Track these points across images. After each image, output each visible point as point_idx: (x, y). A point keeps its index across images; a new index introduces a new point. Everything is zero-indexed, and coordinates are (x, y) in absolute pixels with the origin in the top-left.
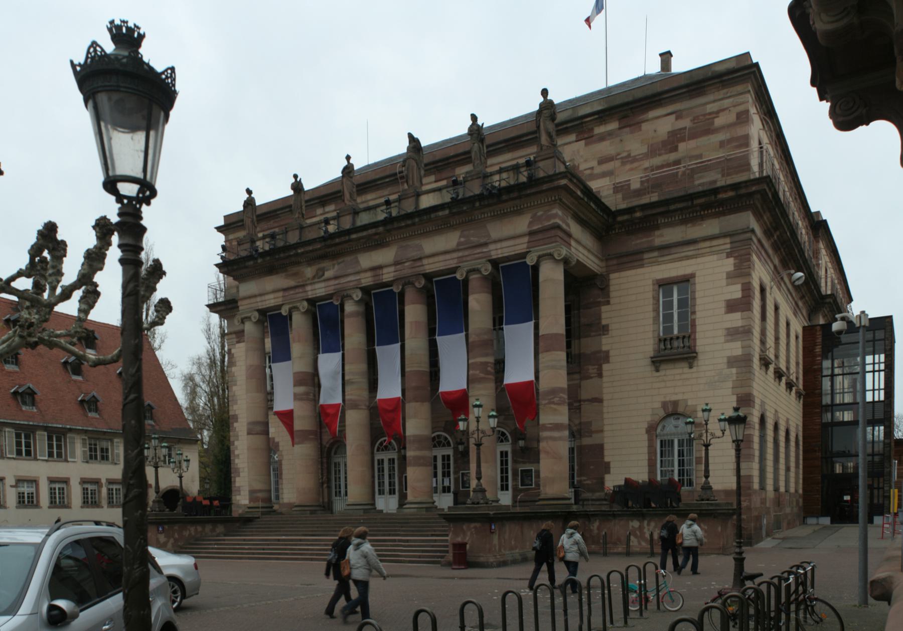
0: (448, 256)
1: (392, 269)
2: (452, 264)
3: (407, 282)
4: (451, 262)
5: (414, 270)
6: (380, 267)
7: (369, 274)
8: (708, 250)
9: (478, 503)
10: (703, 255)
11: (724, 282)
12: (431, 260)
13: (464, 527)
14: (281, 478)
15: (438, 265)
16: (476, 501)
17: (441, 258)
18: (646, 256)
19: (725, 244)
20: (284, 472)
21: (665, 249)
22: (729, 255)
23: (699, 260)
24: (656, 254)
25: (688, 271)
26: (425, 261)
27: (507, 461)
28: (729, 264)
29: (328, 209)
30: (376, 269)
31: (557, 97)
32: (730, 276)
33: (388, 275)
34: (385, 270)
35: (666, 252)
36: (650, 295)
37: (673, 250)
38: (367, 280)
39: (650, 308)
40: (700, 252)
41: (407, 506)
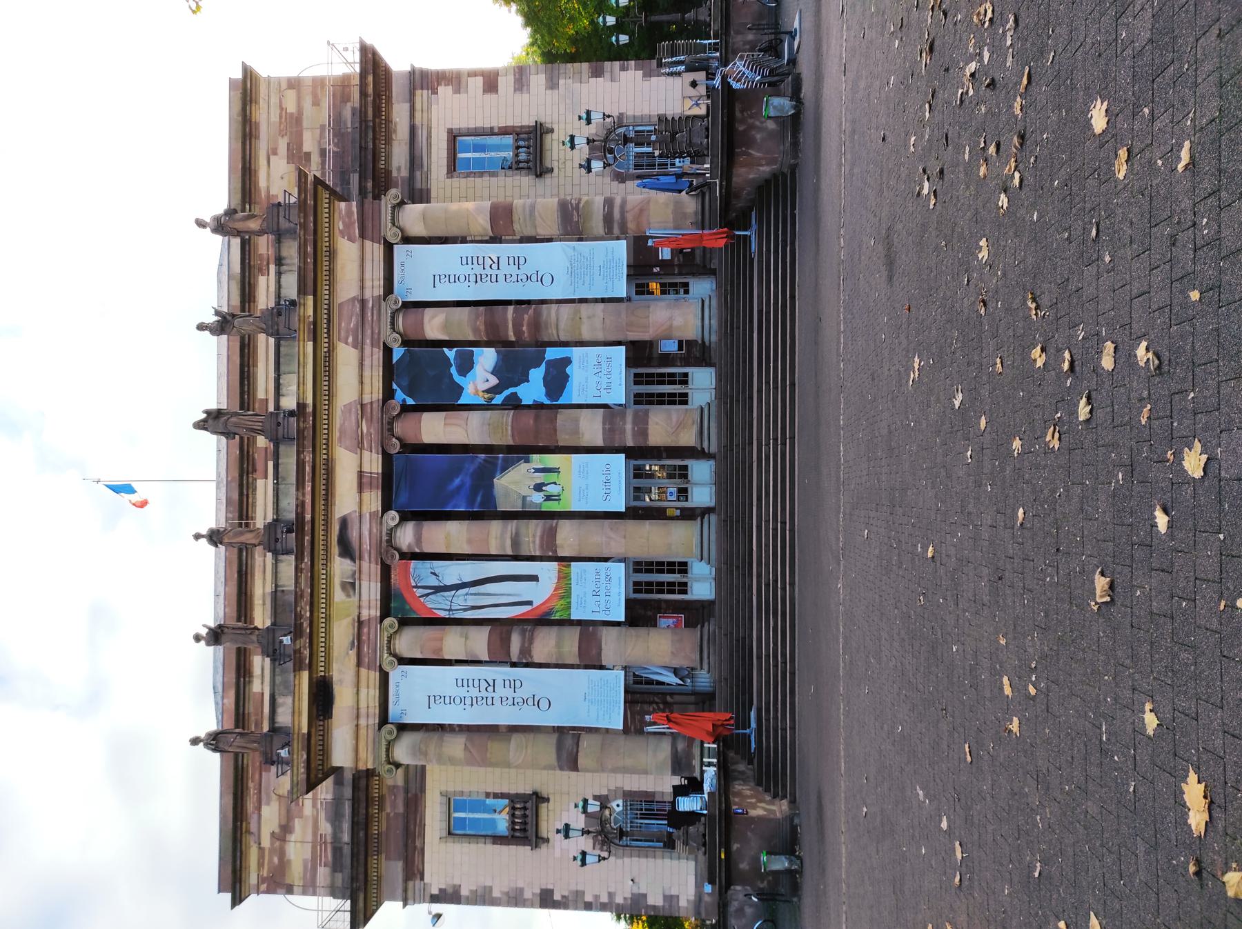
0: (367, 362)
1: (366, 454)
2: (379, 355)
3: (388, 428)
4: (375, 357)
5: (375, 417)
6: (361, 474)
7: (366, 495)
8: (425, 114)
9: (707, 129)
10: (429, 120)
11: (463, 96)
12: (367, 388)
13: (741, 128)
14: (653, 794)
15: (375, 373)
16: (704, 132)
17: (367, 373)
18: (418, 185)
19: (421, 96)
20: (643, 789)
21: (415, 161)
22: (435, 92)
23: (434, 124)
24: (418, 174)
25: (444, 137)
26: (367, 399)
27: (648, 375)
28: (445, 91)
29: (257, 670)
30: (362, 482)
31: (209, 723)
32: (457, 90)
33: (373, 464)
34: (366, 468)
35: (417, 162)
36: (463, 181)
37: (417, 153)
38: (373, 500)
39: (478, 180)
40: (425, 123)
41: (705, 445)
